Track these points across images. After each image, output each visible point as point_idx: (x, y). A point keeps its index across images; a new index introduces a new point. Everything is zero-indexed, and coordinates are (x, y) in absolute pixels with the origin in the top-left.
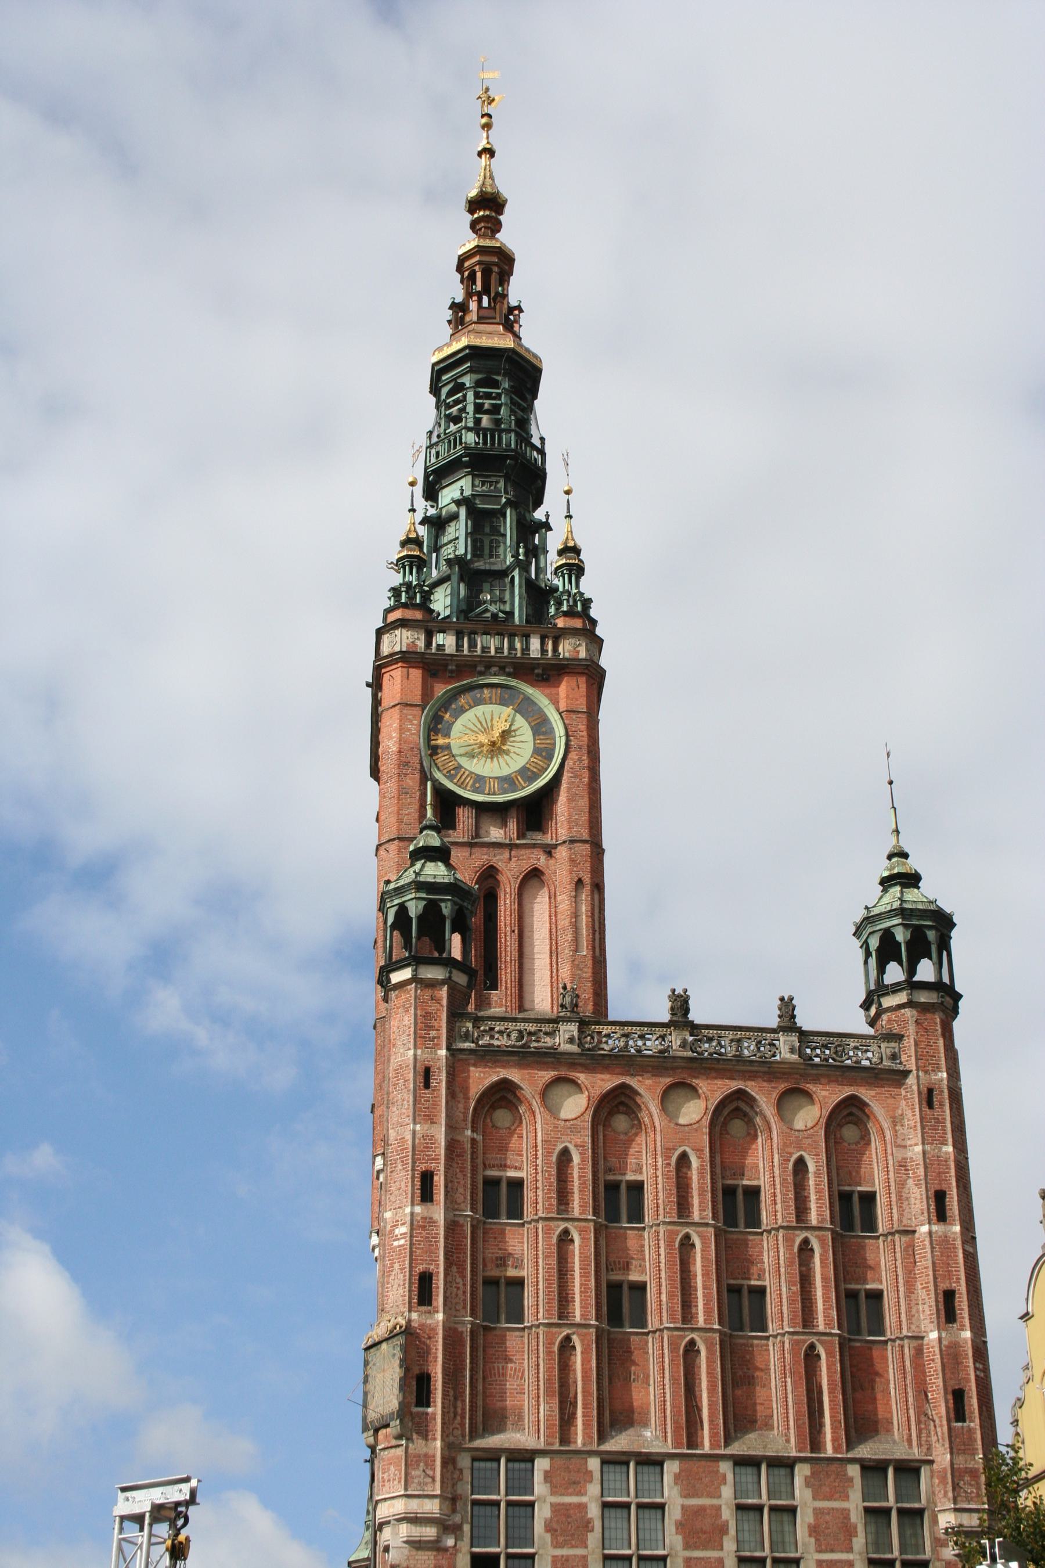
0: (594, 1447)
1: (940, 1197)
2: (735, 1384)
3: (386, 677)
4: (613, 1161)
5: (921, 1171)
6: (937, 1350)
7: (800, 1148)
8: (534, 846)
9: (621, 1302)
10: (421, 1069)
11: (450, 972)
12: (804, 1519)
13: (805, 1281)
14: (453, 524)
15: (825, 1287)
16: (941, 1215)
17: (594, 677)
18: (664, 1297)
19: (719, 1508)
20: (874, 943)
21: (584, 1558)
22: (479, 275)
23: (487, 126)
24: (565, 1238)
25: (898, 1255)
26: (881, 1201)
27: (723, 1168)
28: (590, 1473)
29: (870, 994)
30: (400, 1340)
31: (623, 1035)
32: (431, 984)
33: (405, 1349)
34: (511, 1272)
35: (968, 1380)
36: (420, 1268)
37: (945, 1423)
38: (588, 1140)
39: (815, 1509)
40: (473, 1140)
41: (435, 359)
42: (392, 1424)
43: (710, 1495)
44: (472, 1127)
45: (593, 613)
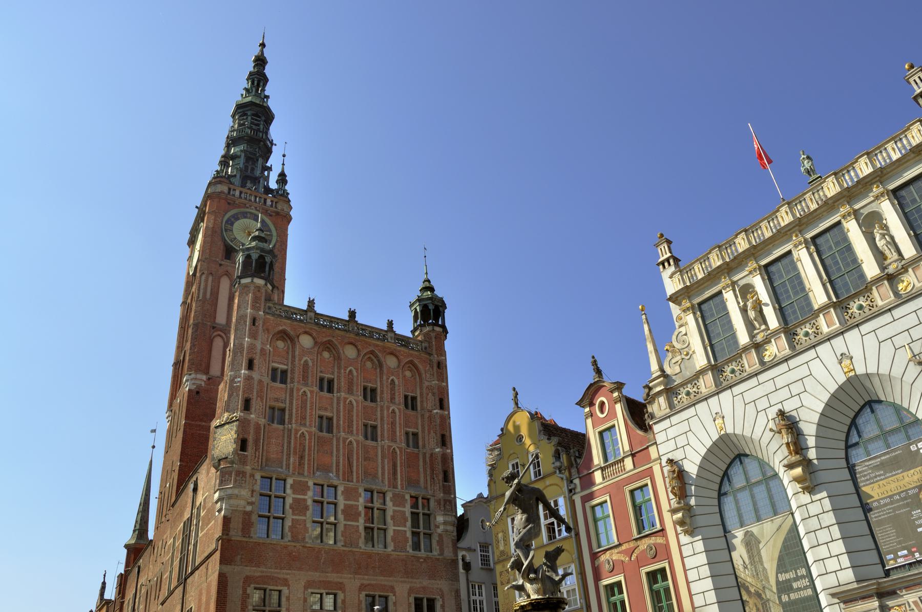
5: (436, 391)
12: (389, 513)
13: (393, 424)
17: (289, 219)
18: (341, 422)
21: (305, 521)
26: (419, 399)
28: (308, 488)
33: (238, 427)
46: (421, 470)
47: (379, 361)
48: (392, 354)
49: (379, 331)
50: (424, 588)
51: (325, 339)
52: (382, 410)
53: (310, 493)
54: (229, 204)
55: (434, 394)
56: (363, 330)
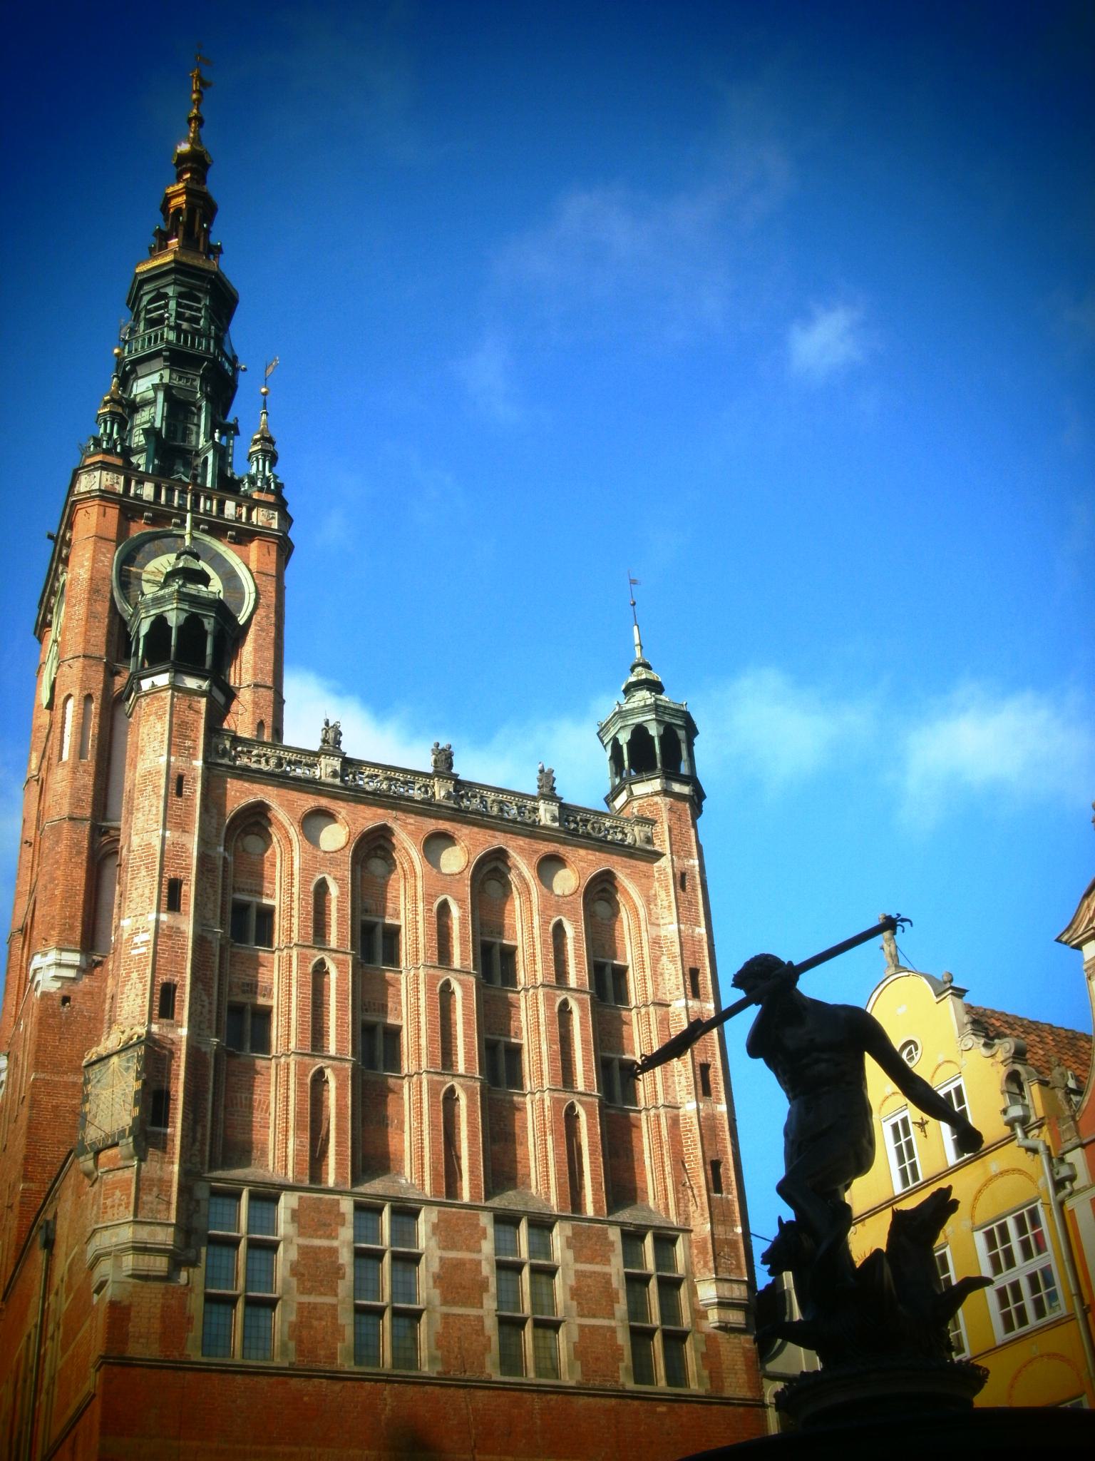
1: (694, 974)
3: (81, 513)
5: (677, 949)
6: (695, 1121)
7: (559, 912)
9: (376, 1045)
10: (174, 776)
14: (147, 409)
15: (584, 1049)
16: (696, 992)
17: (285, 549)
19: (479, 1263)
20: (624, 738)
21: (334, 1307)
25: (654, 1027)
27: (482, 925)
30: (141, 1050)
31: (387, 779)
35: (725, 1153)
37: (704, 1192)
38: (349, 874)
39: (576, 1271)
40: (225, 858)
42: (122, 1142)
43: (469, 1249)
44: (226, 841)
51: (371, 825)
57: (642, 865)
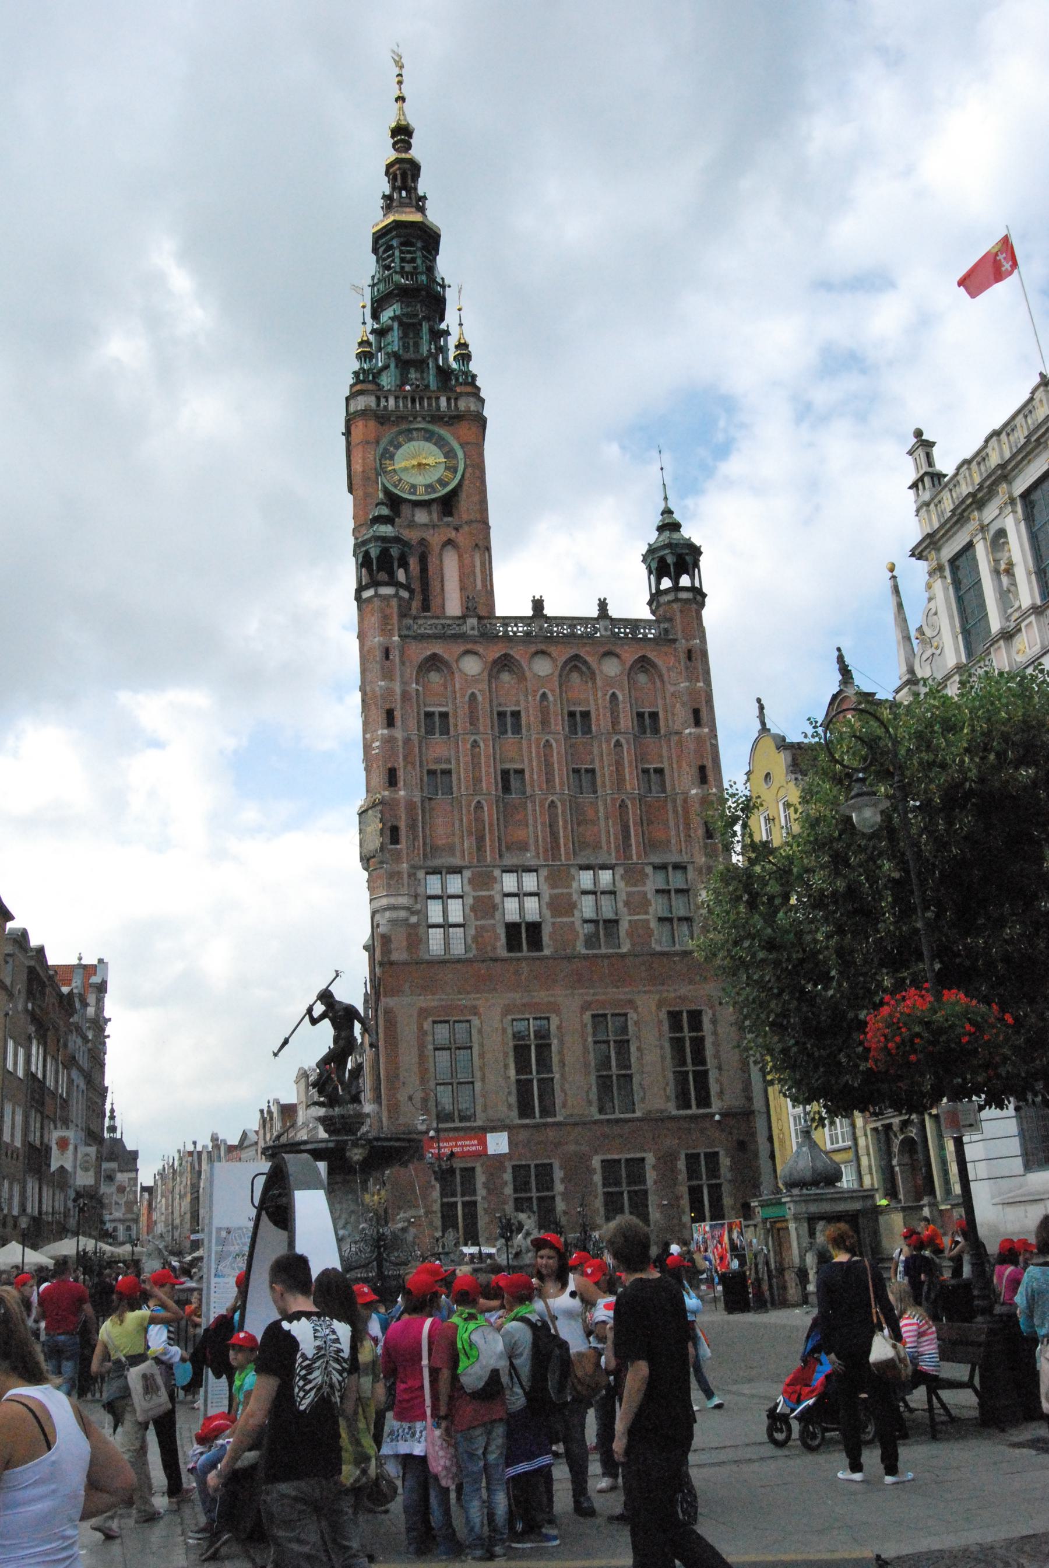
0: (498, 863)
1: (696, 712)
2: (579, 825)
3: (353, 428)
4: (502, 700)
5: (685, 698)
7: (612, 688)
8: (448, 525)
11: (397, 591)
12: (622, 896)
13: (619, 764)
16: (698, 723)
18: (535, 777)
20: (654, 565)
22: (399, 177)
23: (400, 83)
24: (475, 744)
26: (661, 715)
27: (568, 700)
29: (652, 595)
32: (385, 598)
33: (381, 812)
34: (444, 766)
36: (389, 765)
38: (486, 687)
41: (374, 230)
45: (478, 383)
46: (672, 824)
47: (589, 668)
48: (609, 654)
49: (584, 621)
50: (683, 999)
51: (498, 655)
52: (600, 746)
53: (497, 886)
54: (382, 424)
55: (683, 704)
56: (557, 626)
57: (664, 649)
